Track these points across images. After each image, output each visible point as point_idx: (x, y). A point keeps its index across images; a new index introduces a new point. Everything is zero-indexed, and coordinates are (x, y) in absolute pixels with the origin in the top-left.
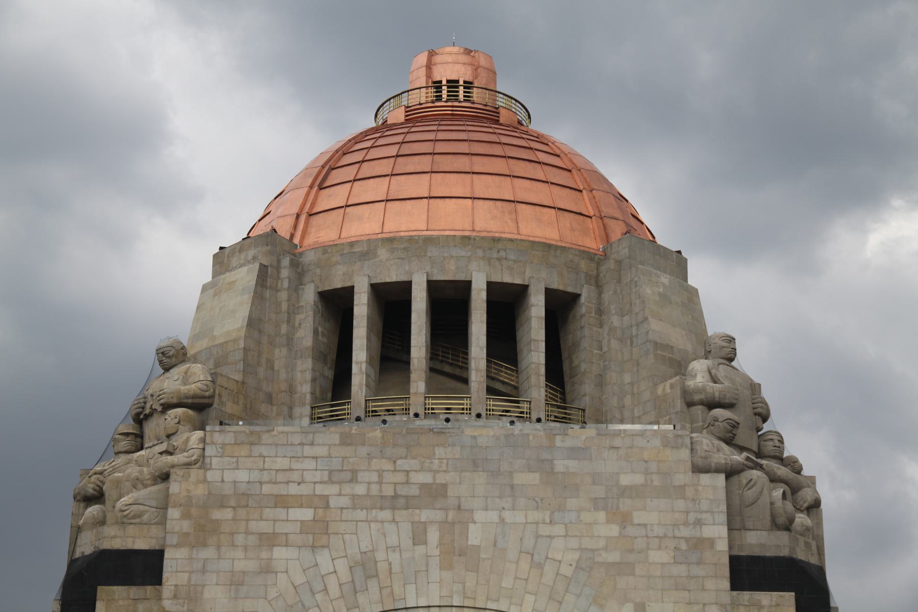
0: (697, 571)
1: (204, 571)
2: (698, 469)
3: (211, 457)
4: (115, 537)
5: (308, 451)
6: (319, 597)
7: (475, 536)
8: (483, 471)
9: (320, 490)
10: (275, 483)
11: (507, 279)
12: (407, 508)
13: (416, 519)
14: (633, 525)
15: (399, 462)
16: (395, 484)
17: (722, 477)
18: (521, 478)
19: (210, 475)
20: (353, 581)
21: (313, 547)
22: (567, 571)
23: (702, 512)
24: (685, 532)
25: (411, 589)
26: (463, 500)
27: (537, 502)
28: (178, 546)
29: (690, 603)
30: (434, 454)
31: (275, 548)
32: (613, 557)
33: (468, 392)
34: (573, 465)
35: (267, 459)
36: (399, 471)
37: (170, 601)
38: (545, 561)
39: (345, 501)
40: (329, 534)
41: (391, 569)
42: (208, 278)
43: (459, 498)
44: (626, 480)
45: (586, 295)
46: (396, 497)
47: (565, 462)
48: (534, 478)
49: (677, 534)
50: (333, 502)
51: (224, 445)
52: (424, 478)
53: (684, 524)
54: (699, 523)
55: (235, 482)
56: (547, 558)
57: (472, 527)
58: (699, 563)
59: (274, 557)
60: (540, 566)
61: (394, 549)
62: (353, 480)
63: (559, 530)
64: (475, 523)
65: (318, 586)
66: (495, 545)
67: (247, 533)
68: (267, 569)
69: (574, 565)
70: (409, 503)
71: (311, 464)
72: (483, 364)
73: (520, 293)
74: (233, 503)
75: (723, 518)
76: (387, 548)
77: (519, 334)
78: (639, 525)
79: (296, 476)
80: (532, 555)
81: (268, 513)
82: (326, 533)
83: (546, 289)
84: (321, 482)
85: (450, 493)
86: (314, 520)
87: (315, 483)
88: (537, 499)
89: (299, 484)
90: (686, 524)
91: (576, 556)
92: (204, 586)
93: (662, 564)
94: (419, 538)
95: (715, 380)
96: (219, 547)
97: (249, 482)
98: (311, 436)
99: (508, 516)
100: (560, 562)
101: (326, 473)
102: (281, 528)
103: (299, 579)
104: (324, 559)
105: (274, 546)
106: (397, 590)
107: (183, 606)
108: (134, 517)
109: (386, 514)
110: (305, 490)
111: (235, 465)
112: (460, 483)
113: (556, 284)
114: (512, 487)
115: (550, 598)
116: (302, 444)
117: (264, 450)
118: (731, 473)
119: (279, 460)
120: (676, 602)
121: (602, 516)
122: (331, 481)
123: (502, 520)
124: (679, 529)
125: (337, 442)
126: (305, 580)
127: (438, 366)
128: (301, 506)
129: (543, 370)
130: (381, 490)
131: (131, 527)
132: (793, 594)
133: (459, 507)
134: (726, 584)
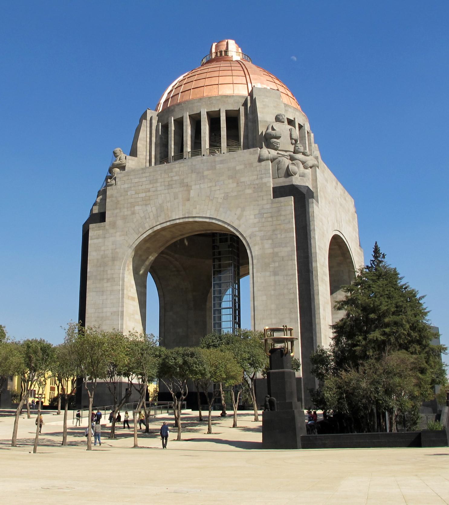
1: (116, 216)
2: (260, 160)
3: (117, 182)
5: (144, 175)
7: (192, 193)
8: (195, 173)
9: (147, 186)
15: (170, 174)
16: (169, 181)
18: (206, 173)
21: (146, 205)
22: (220, 201)
23: (262, 174)
24: (257, 182)
26: (188, 183)
32: (235, 194)
34: (221, 165)
35: (133, 180)
38: (213, 198)
41: (168, 208)
43: (187, 182)
44: (238, 168)
47: (219, 165)
49: (255, 183)
50: (151, 190)
53: (257, 179)
54: (262, 178)
55: (124, 188)
56: (214, 197)
57: (191, 191)
58: (261, 191)
60: (212, 200)
61: (169, 202)
63: (218, 188)
65: (147, 216)
68: (133, 213)
69: (222, 198)
71: (144, 179)
76: (167, 202)
79: (141, 184)
80: (209, 197)
86: (146, 196)
87: (146, 185)
88: (211, 179)
90: (257, 179)
91: (223, 195)
96: (120, 208)
97: (128, 188)
98: (144, 171)
99: (202, 186)
100: (218, 198)
101: (149, 181)
103: (142, 215)
104: (149, 208)
106: (170, 215)
110: (144, 187)
111: (124, 183)
113: (230, 108)
114: (203, 176)
115: (215, 210)
117: (132, 177)
118: (273, 160)
119: (136, 179)
120: (254, 205)
121: (231, 181)
122: (150, 183)
126: (144, 215)
128: (142, 193)
133: (187, 185)
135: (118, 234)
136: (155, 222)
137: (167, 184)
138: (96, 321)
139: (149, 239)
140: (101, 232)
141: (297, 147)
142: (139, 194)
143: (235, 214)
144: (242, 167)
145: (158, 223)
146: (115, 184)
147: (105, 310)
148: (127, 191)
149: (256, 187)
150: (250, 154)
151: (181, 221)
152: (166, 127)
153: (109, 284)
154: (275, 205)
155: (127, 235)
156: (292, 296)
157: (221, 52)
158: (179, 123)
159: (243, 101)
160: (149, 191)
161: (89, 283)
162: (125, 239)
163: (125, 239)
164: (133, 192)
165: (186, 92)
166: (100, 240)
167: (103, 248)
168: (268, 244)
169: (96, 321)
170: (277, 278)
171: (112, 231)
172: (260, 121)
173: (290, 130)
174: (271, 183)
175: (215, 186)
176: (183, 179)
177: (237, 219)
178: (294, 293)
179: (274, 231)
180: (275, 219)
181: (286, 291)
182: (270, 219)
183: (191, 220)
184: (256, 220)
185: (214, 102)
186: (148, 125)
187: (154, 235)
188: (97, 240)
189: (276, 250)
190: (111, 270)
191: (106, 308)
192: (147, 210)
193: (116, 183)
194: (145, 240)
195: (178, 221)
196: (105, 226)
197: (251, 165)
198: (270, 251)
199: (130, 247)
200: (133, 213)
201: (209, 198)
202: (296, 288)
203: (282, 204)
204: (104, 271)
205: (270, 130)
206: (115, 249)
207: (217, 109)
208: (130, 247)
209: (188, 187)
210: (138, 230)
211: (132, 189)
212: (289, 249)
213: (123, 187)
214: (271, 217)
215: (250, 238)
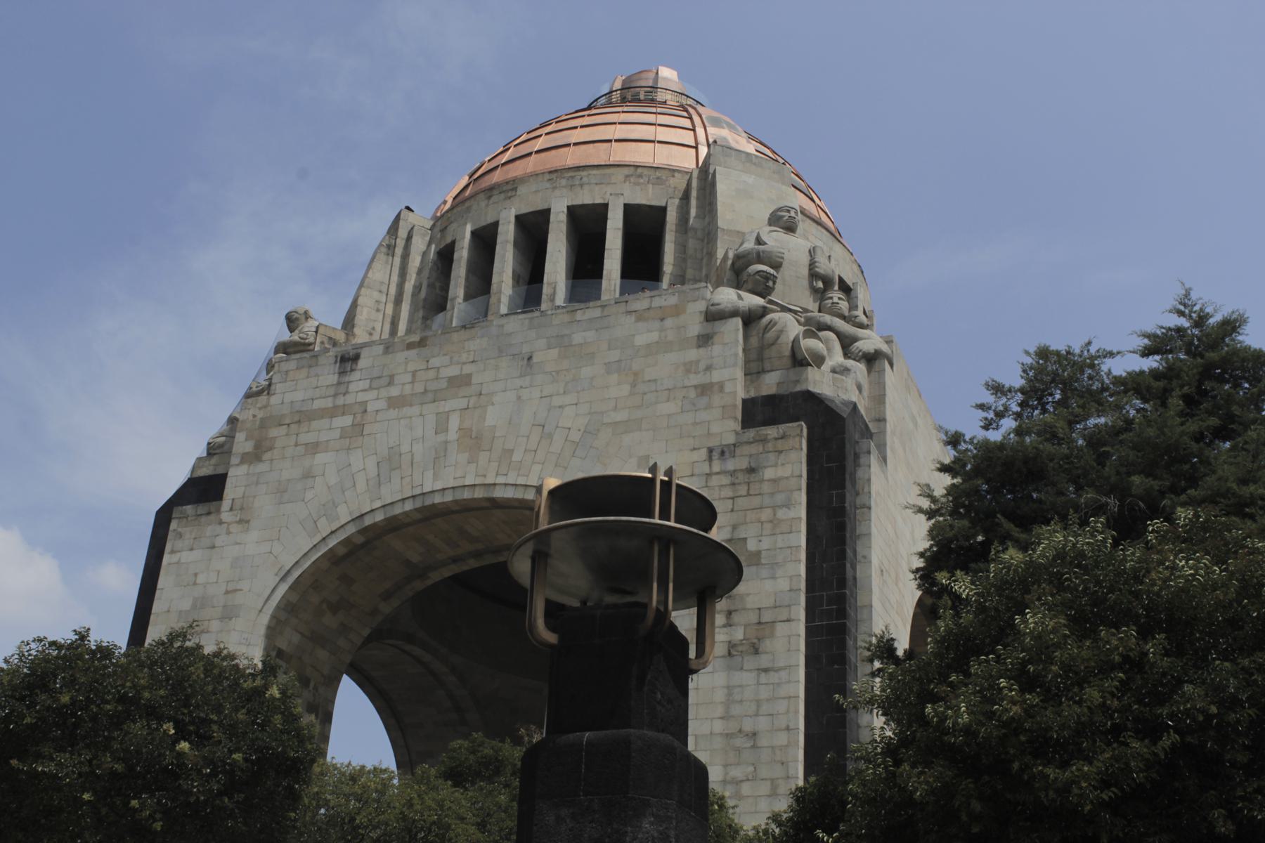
0: (703, 416)
1: (257, 483)
9: (362, 397)
12: (434, 401)
13: (441, 410)
14: (644, 382)
19: (274, 400)
20: (378, 475)
22: (575, 436)
24: (695, 379)
25: (430, 474)
27: (553, 376)
28: (242, 462)
29: (694, 449)
30: (464, 348)
31: (318, 456)
34: (590, 335)
36: (431, 369)
37: (227, 513)
39: (381, 404)
40: (364, 436)
44: (640, 340)
46: (426, 391)
48: (554, 353)
49: (687, 383)
50: (369, 408)
51: (287, 372)
52: (453, 371)
54: (709, 368)
57: (490, 408)
59: (315, 463)
62: (390, 384)
64: (493, 404)
66: (510, 423)
67: (296, 445)
69: (582, 430)
70: (437, 396)
73: (601, 212)
74: (287, 422)
78: (649, 381)
80: (544, 426)
81: (315, 424)
82: (362, 435)
84: (362, 391)
85: (474, 380)
86: (352, 425)
88: (554, 373)
89: (344, 394)
92: (255, 497)
93: (669, 416)
94: (441, 427)
97: (303, 401)
100: (570, 429)
101: (368, 381)
102: (323, 437)
104: (356, 459)
105: (315, 454)
107: (237, 516)
108: (214, 450)
109: (415, 410)
112: (484, 370)
118: (750, 319)
122: (371, 388)
123: (519, 398)
124: (688, 378)
125: (381, 352)
128: (343, 414)
130: (413, 389)
133: (481, 394)
139: (350, 554)
141: (830, 301)
145: (378, 504)
152: (446, 256)
156: (782, 739)
158: (485, 240)
162: (271, 552)
163: (271, 552)
165: (518, 162)
166: (197, 554)
173: (810, 251)
180: (742, 490)
181: (763, 724)
187: (363, 546)
188: (189, 552)
194: (332, 558)
195: (438, 499)
200: (308, 475)
201: (543, 430)
202: (797, 712)
203: (770, 446)
210: (315, 522)
212: (783, 584)
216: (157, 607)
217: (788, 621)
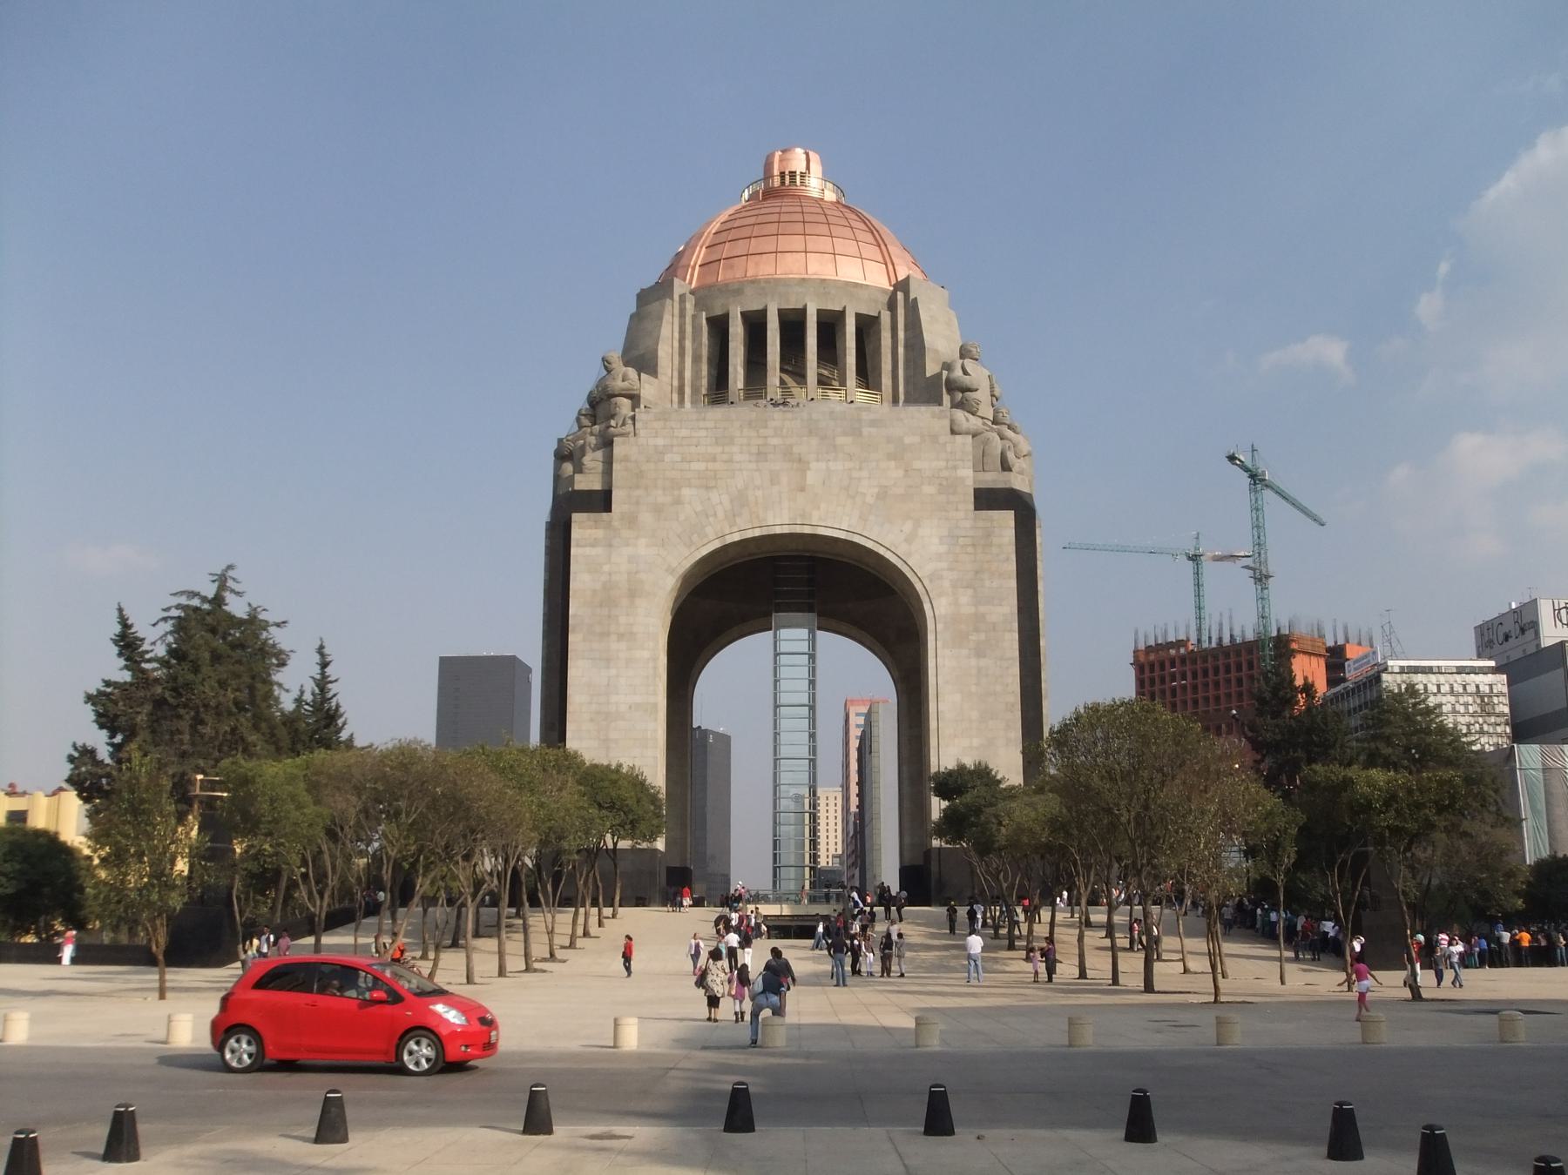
4: (581, 482)
5: (702, 424)
6: (711, 519)
7: (811, 478)
9: (710, 450)
10: (681, 445)
11: (830, 307)
16: (759, 445)
17: (971, 437)
18: (840, 440)
22: (870, 500)
24: (945, 473)
33: (806, 384)
34: (873, 430)
42: (634, 309)
43: (799, 454)
44: (907, 440)
45: (886, 318)
54: (955, 468)
55: (656, 446)
57: (809, 473)
63: (864, 474)
64: (809, 469)
68: (678, 501)
71: (703, 433)
72: (815, 364)
75: (971, 464)
77: (838, 345)
83: (856, 314)
86: (707, 470)
87: (706, 445)
90: (947, 468)
91: (876, 490)
93: (931, 495)
94: (774, 480)
95: (965, 372)
97: (664, 446)
101: (714, 439)
103: (699, 508)
104: (714, 496)
113: (864, 311)
114: (835, 446)
115: (860, 517)
116: (698, 420)
119: (683, 430)
121: (893, 464)
127: (786, 367)
128: (699, 461)
129: (854, 368)
131: (591, 475)
132: (1013, 512)
133: (800, 460)
134: (972, 507)
135: (643, 541)
136: (728, 527)
137: (754, 450)
138: (592, 720)
140: (600, 533)
141: (1001, 415)
142: (692, 464)
143: (902, 531)
144: (917, 439)
146: (632, 434)
147: (614, 699)
148: (662, 453)
149: (945, 483)
150: (934, 416)
151: (786, 530)
153: (623, 645)
154: (981, 524)
155: (663, 546)
157: (793, 174)
159: (886, 298)
160: (714, 460)
161: (574, 639)
162: (658, 555)
163: (658, 555)
164: (678, 458)
166: (598, 551)
167: (606, 568)
168: (965, 598)
169: (592, 720)
170: (983, 662)
171: (625, 533)
172: (929, 349)
174: (968, 478)
175: (860, 469)
176: (791, 446)
177: (906, 540)
178: (1013, 692)
179: (977, 572)
181: (998, 688)
182: (970, 549)
183: (807, 530)
184: (943, 549)
185: (833, 292)
186: (676, 311)
189: (982, 609)
190: (628, 615)
191: (617, 694)
192: (709, 499)
193: (637, 432)
195: (778, 530)
196: (611, 522)
197: (934, 438)
198: (971, 610)
199: (671, 571)
203: (995, 524)
204: (609, 617)
205: (958, 373)
206: (636, 573)
207: (838, 308)
208: (671, 571)
209: (801, 464)
211: (675, 449)
213: (652, 442)
214: (974, 545)
215: (931, 581)
216: (574, 585)
217: (1010, 631)
